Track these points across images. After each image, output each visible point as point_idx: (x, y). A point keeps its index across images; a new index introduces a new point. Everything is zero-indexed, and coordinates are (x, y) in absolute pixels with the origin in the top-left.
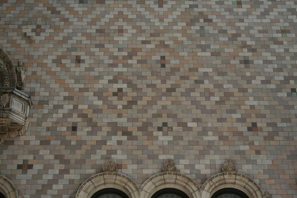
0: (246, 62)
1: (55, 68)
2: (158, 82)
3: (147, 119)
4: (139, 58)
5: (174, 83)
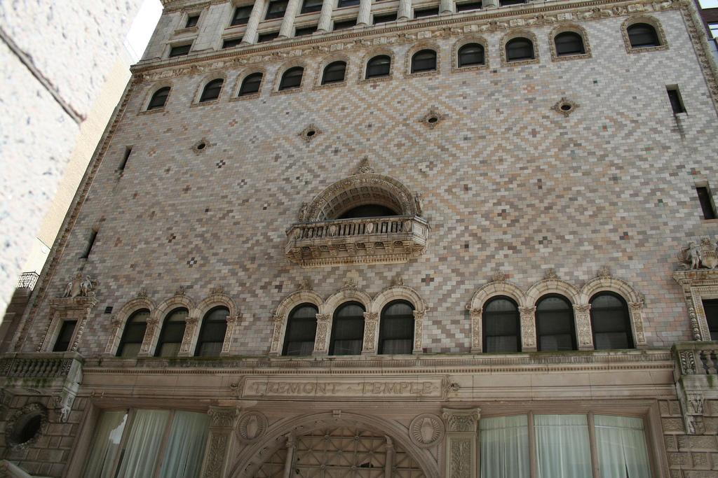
0: (615, 179)
1: (447, 196)
2: (536, 202)
3: (529, 234)
4: (519, 182)
5: (550, 201)
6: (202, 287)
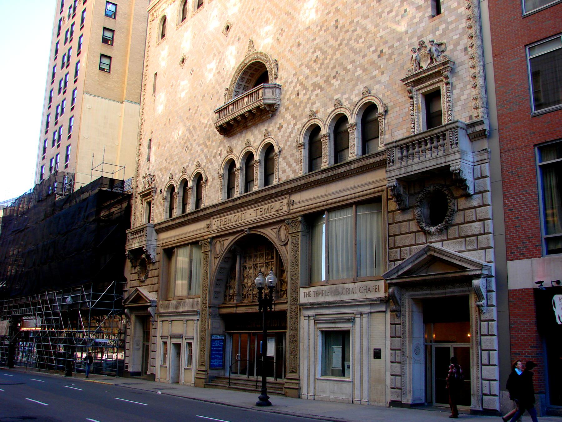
6: (192, 164)
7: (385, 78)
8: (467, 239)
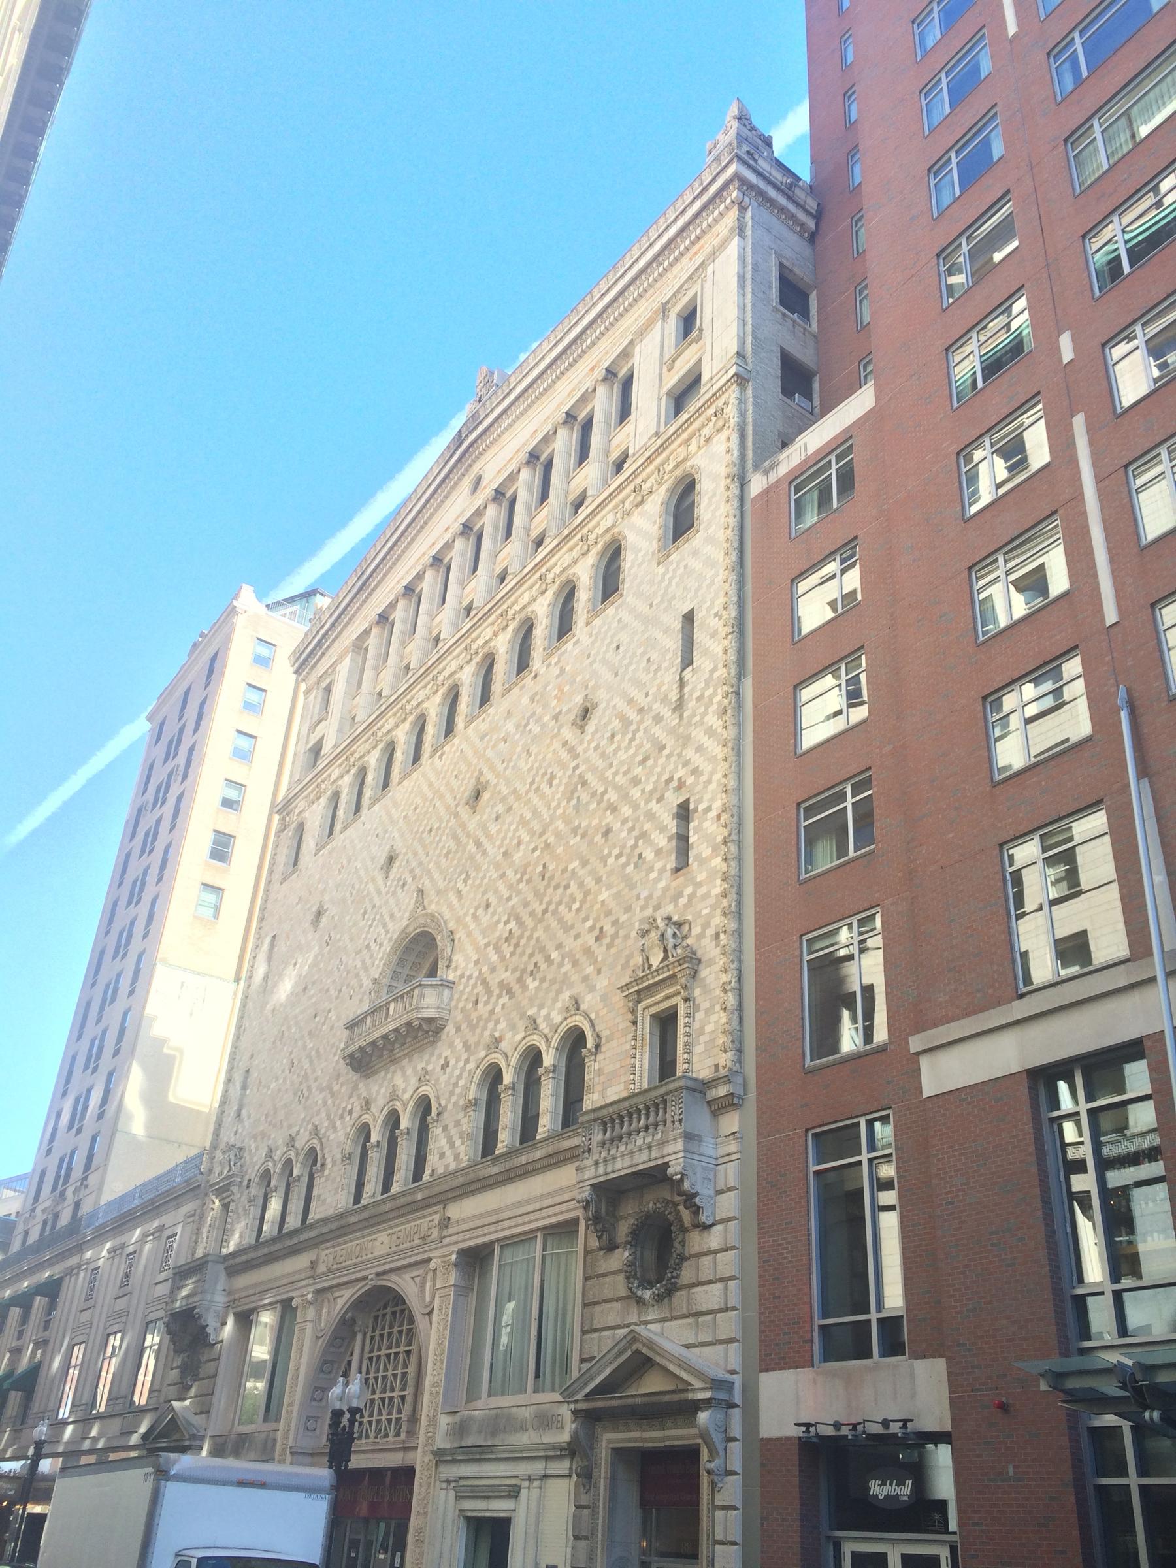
7: (602, 983)
8: (701, 1319)
